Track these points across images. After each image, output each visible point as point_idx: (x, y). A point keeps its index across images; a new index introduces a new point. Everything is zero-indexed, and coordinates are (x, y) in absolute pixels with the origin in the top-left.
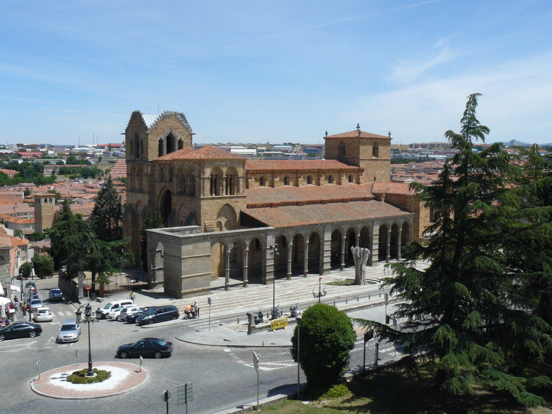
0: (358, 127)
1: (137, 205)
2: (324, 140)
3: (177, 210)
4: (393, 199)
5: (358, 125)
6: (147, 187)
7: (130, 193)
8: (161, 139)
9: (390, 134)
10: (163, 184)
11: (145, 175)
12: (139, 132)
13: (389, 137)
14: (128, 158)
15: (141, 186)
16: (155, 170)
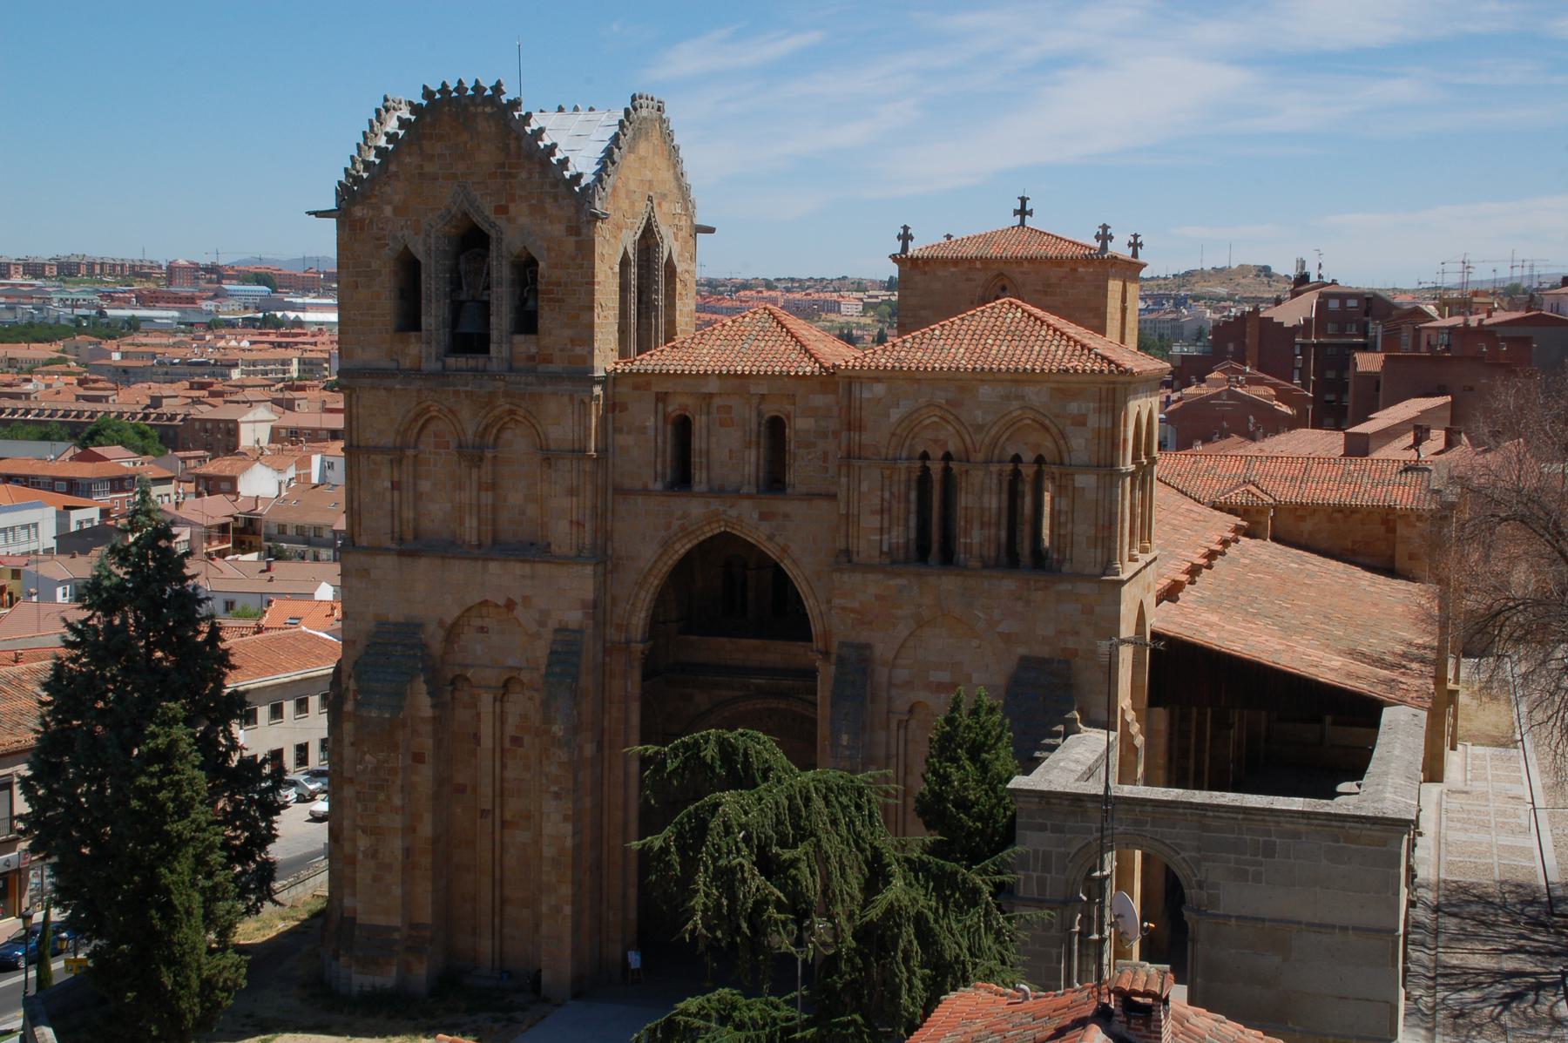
0: (1023, 212)
1: (452, 632)
2: (896, 267)
3: (883, 649)
4: (1307, 526)
5: (1023, 200)
6: (579, 524)
7: (385, 566)
8: (626, 253)
9: (1135, 245)
10: (696, 508)
11: (548, 456)
12: (502, 210)
13: (1135, 255)
14: (369, 356)
15: (494, 522)
16: (617, 430)
